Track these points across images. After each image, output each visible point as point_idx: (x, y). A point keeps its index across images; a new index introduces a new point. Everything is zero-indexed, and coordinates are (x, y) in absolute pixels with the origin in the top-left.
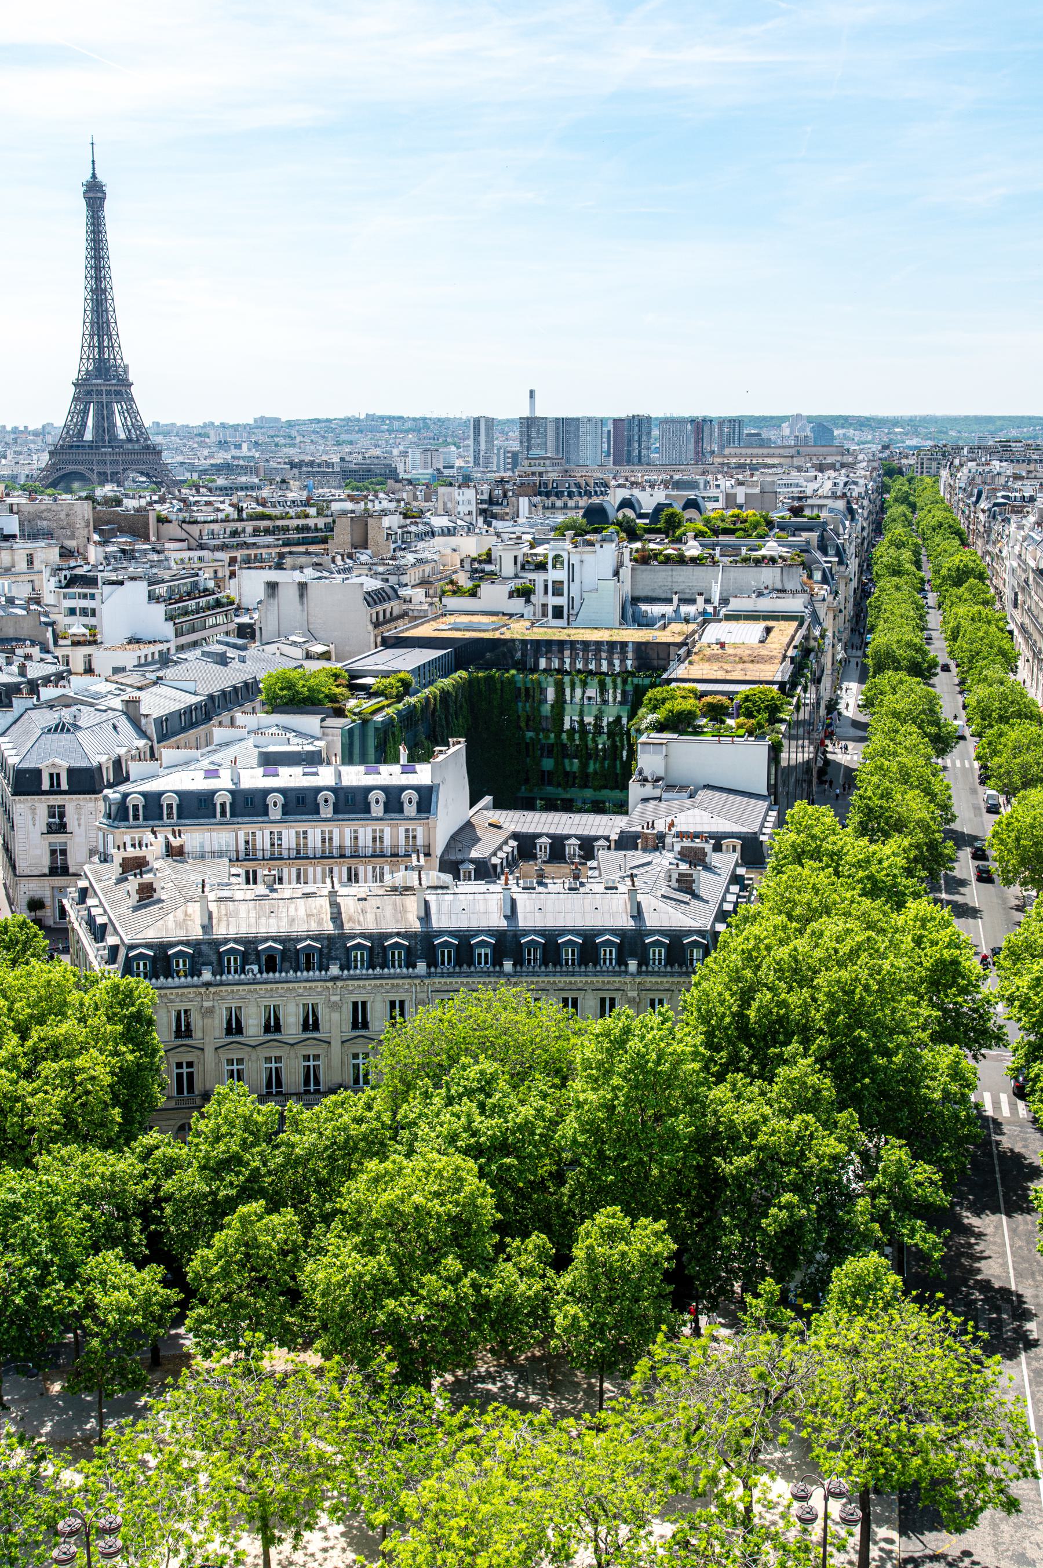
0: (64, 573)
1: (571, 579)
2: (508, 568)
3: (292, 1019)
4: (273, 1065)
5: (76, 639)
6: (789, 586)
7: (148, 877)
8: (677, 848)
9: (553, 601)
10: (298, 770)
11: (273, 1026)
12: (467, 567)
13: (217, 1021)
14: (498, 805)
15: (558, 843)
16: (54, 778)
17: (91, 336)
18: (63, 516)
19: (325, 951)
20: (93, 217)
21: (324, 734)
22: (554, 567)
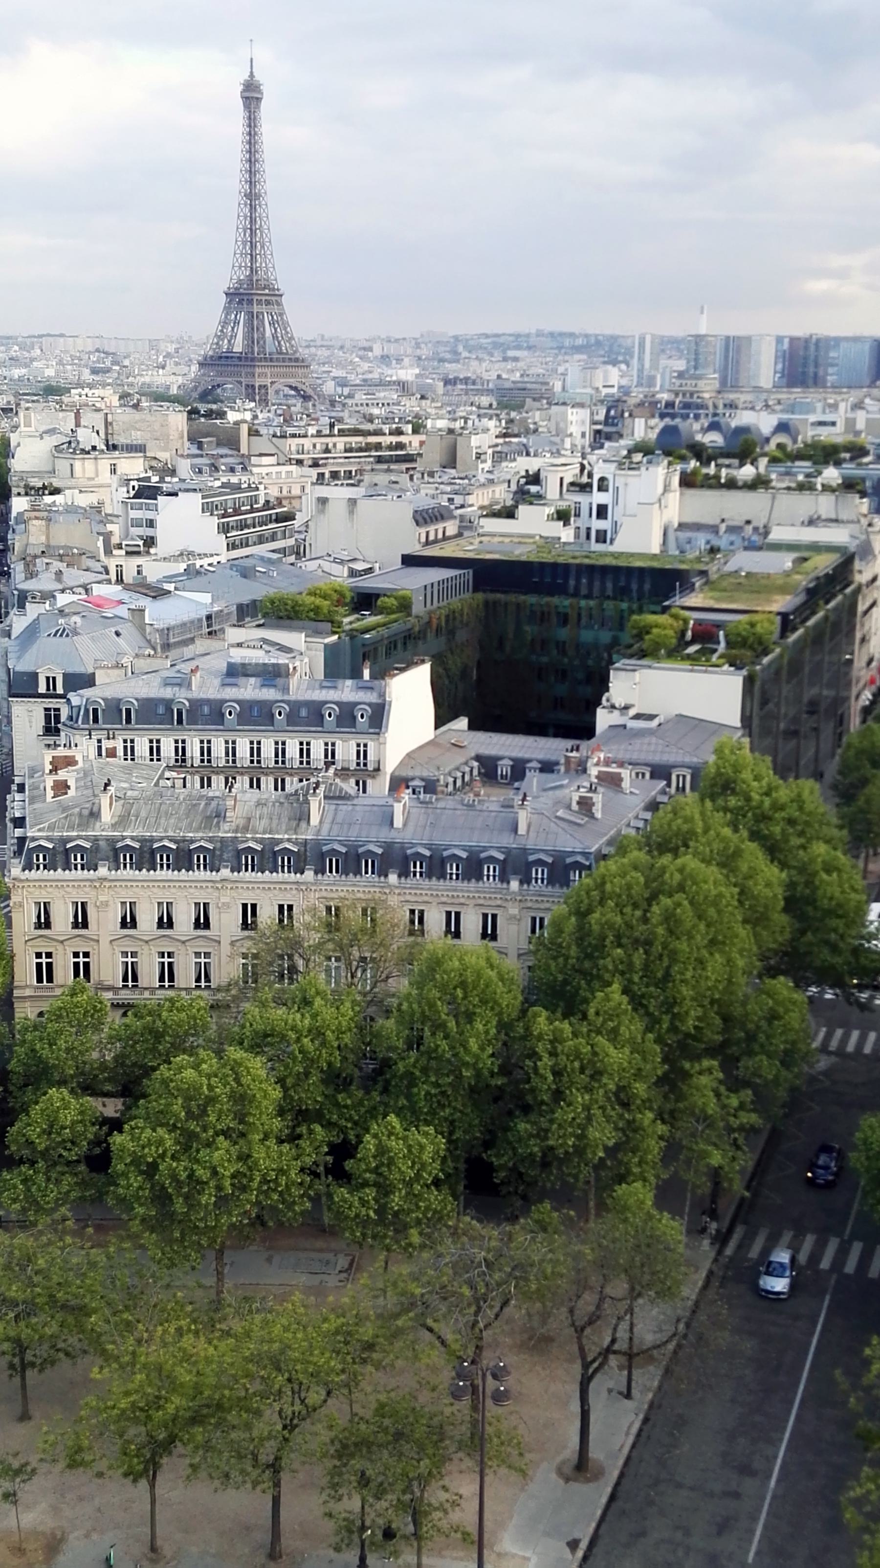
0: (132, 483)
1: (616, 502)
3: (184, 918)
4: (130, 960)
5: (130, 549)
6: (843, 516)
7: (62, 775)
9: (598, 525)
11: (166, 922)
13: (111, 915)
16: (51, 682)
17: (244, 243)
18: (157, 426)
19: (218, 853)
20: (250, 118)
21: (308, 648)
22: (600, 489)
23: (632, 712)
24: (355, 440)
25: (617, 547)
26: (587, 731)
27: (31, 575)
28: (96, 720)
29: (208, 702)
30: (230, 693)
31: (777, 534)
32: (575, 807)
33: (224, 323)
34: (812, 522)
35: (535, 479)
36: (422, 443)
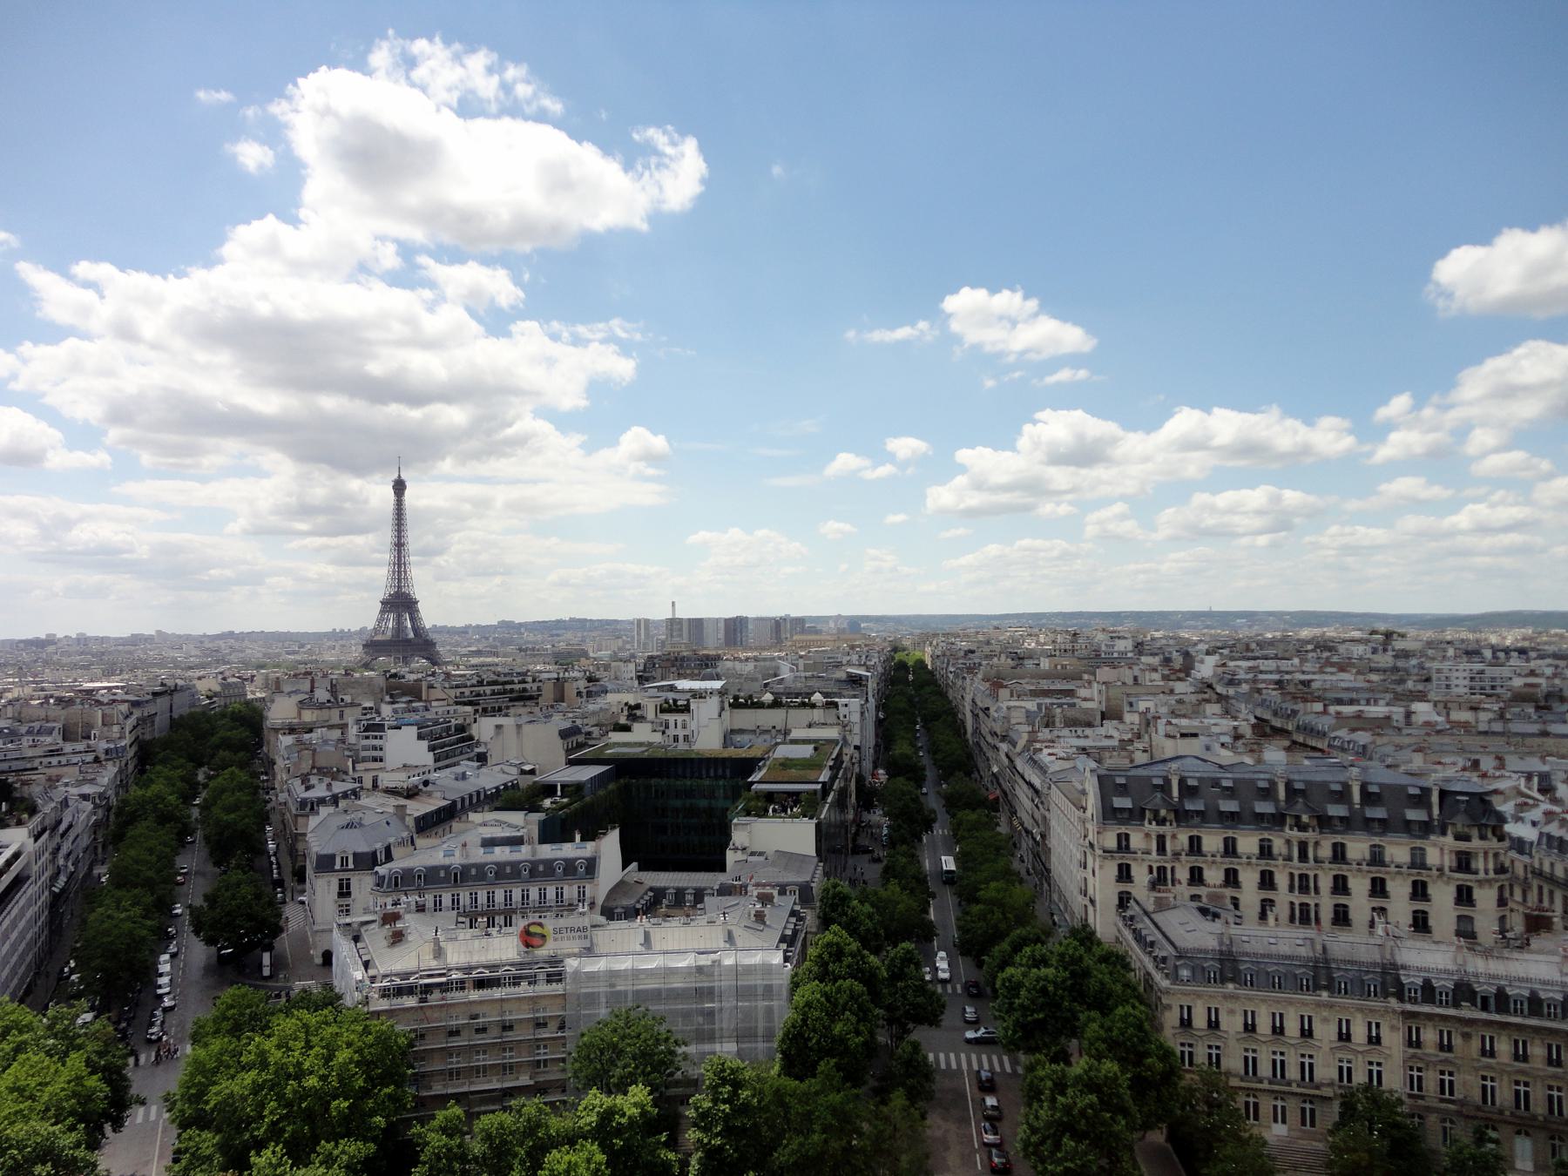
2: (650, 715)
7: (399, 925)
8: (755, 893)
10: (507, 849)
12: (626, 713)
14: (641, 869)
15: (680, 893)
16: (344, 860)
17: (394, 572)
23: (749, 851)
24: (496, 688)
25: (695, 747)
26: (721, 867)
27: (308, 788)
28: (396, 885)
29: (474, 865)
30: (490, 858)
31: (795, 734)
32: (753, 919)
33: (380, 621)
34: (810, 726)
35: (638, 706)
36: (539, 689)
